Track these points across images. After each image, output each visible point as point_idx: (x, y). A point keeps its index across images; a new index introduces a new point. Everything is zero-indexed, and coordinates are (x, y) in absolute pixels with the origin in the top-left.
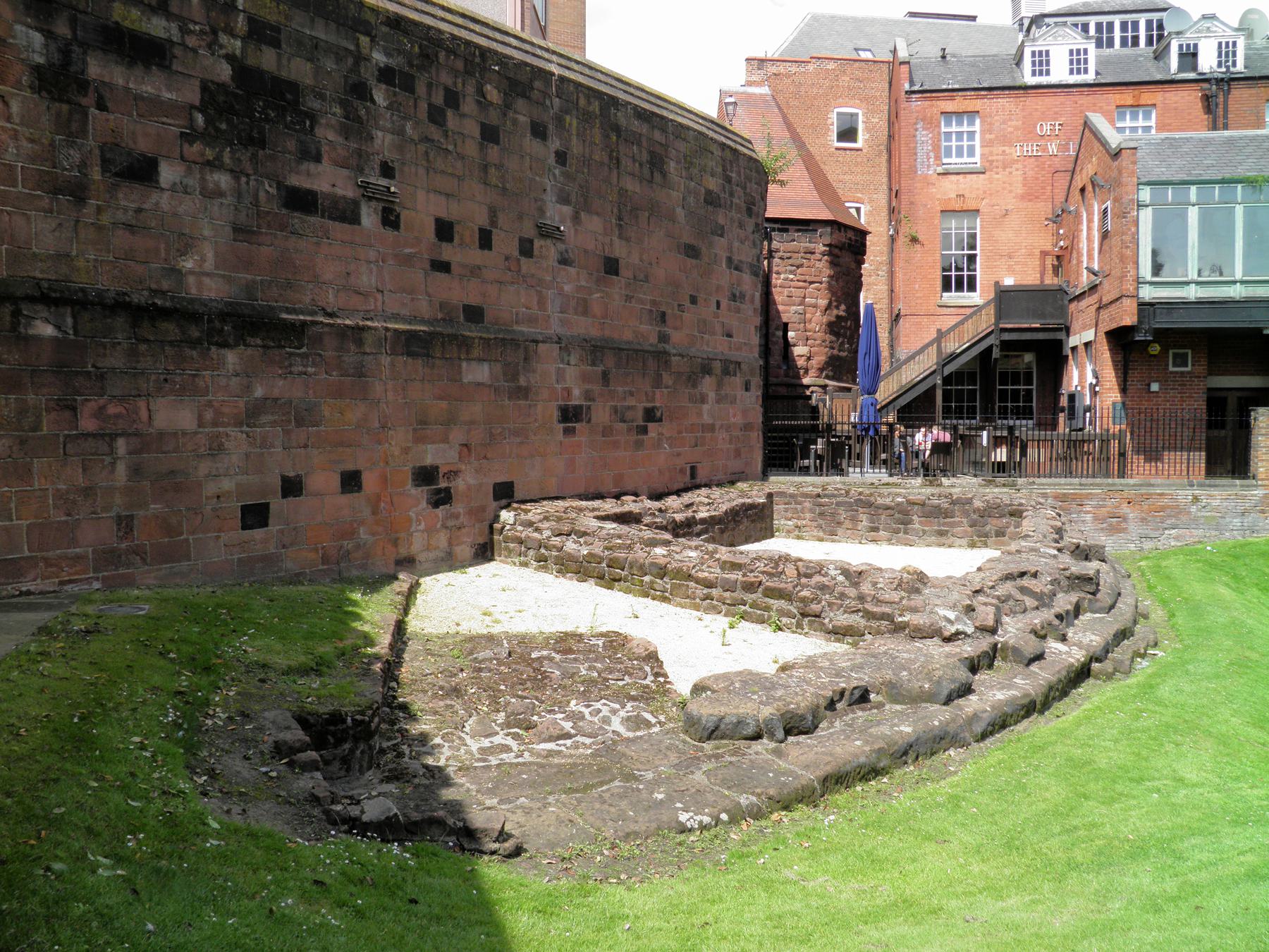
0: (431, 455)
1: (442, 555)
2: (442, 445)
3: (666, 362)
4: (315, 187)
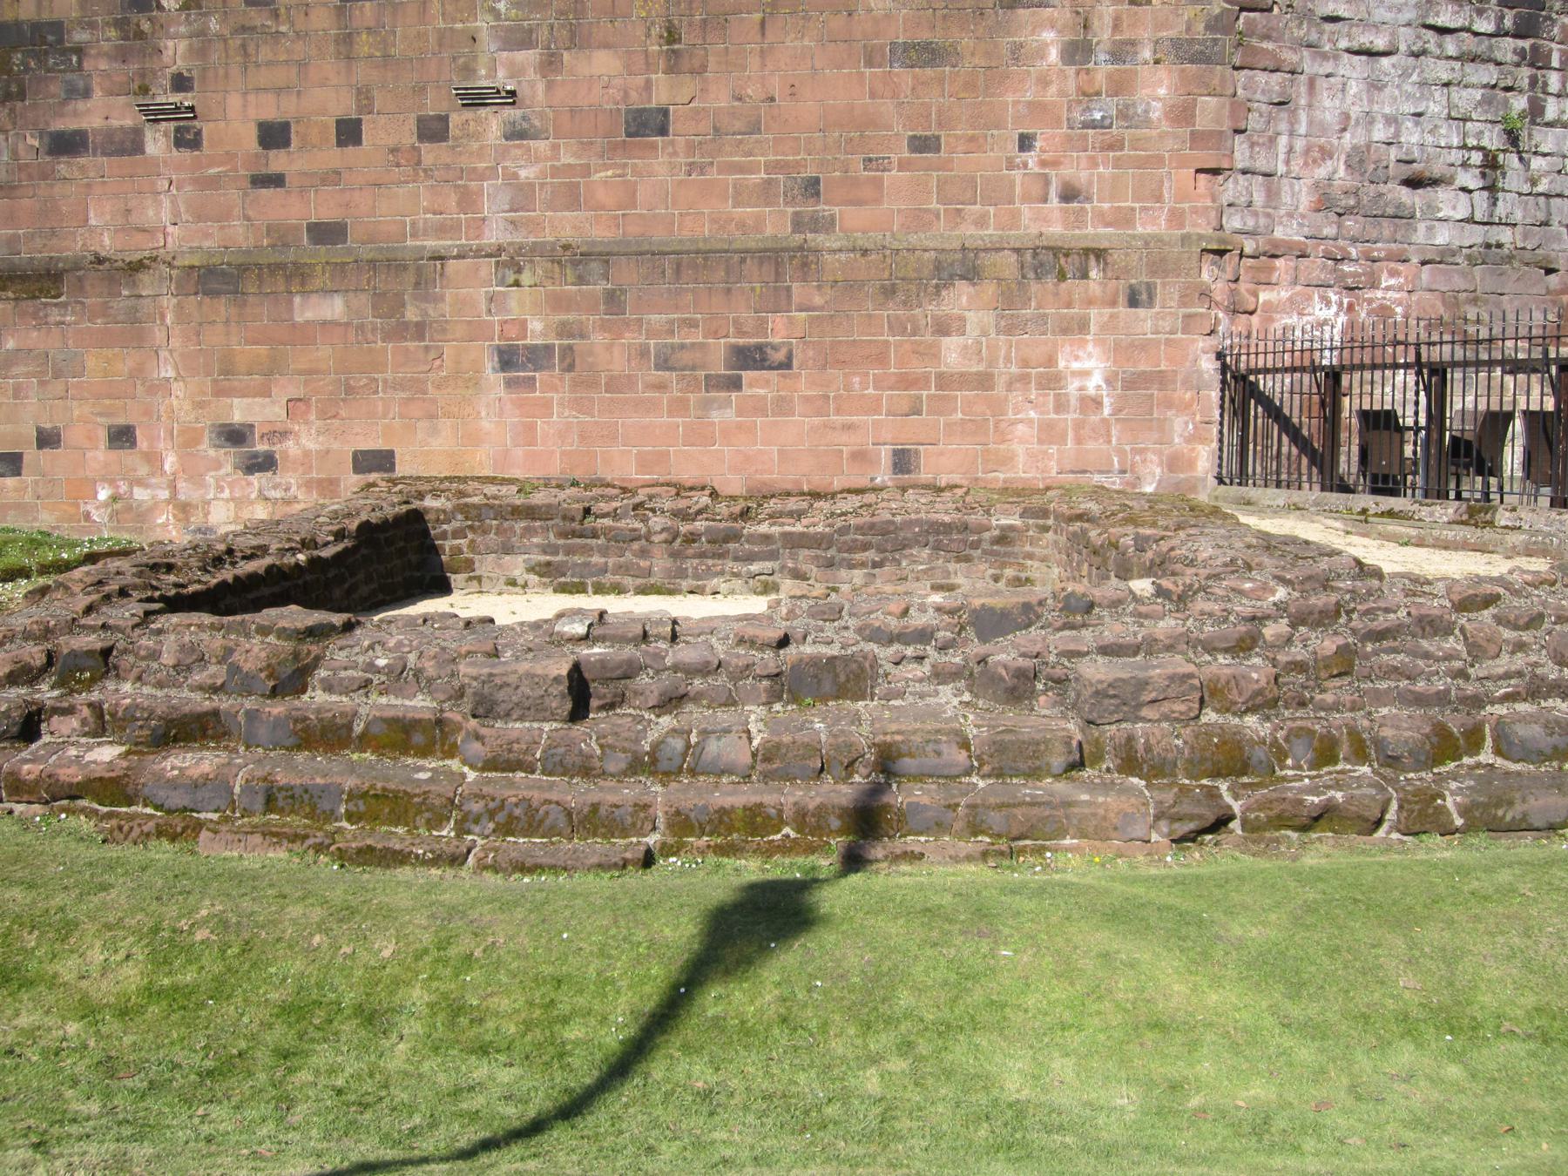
0: (239, 412)
3: (805, 265)
4: (84, 125)
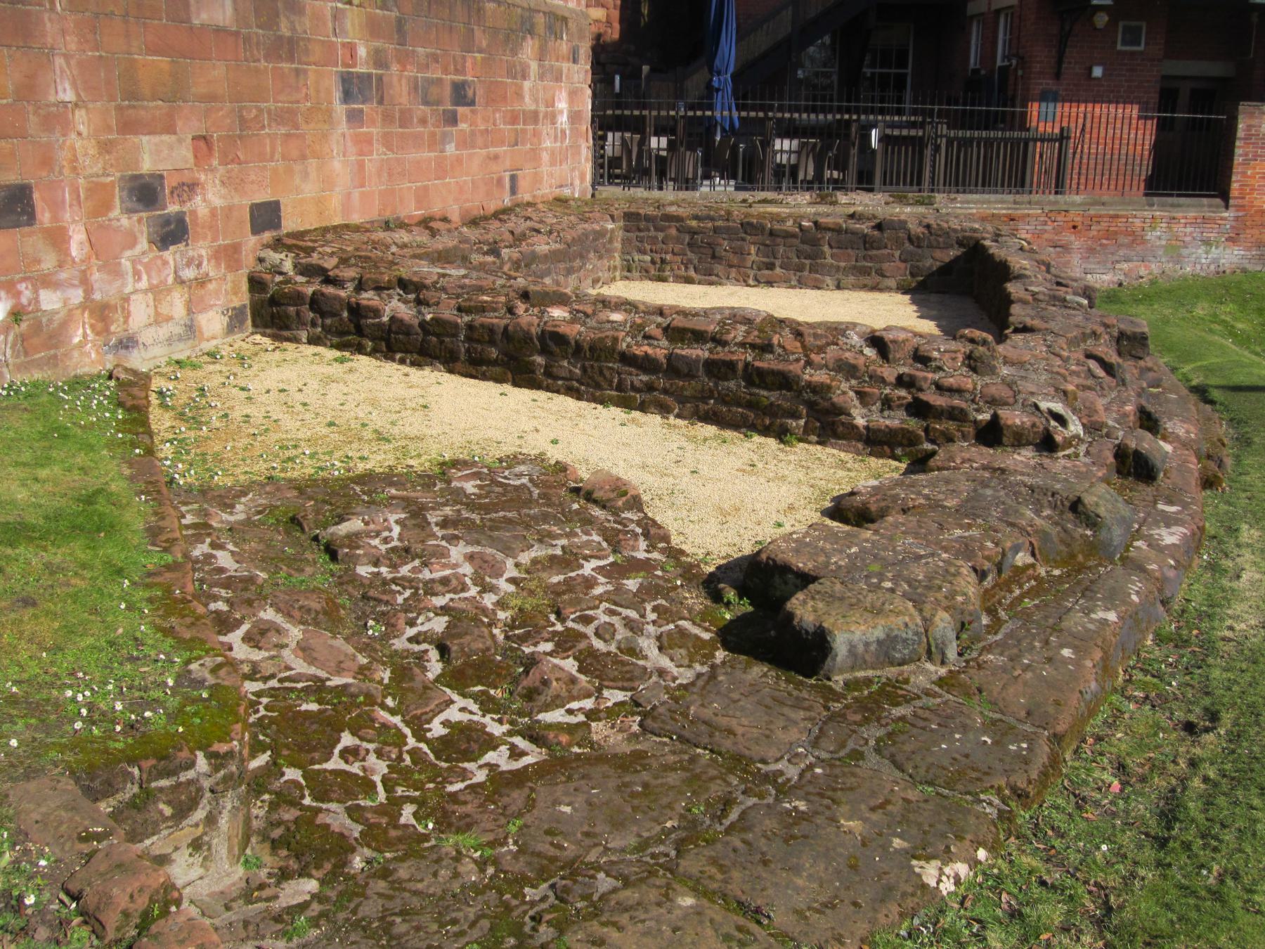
1: (178, 330)
2: (165, 138)
3: (479, 10)
